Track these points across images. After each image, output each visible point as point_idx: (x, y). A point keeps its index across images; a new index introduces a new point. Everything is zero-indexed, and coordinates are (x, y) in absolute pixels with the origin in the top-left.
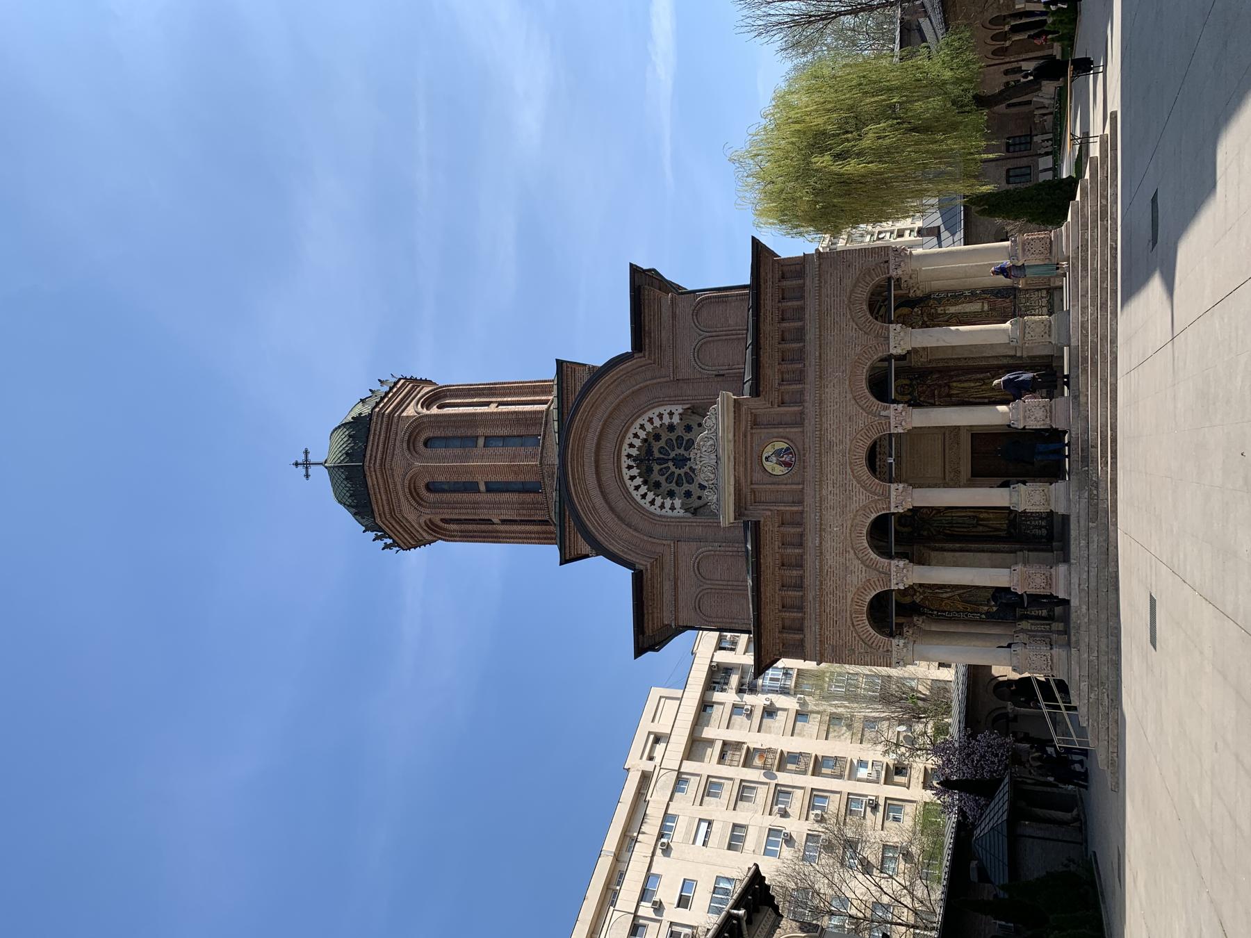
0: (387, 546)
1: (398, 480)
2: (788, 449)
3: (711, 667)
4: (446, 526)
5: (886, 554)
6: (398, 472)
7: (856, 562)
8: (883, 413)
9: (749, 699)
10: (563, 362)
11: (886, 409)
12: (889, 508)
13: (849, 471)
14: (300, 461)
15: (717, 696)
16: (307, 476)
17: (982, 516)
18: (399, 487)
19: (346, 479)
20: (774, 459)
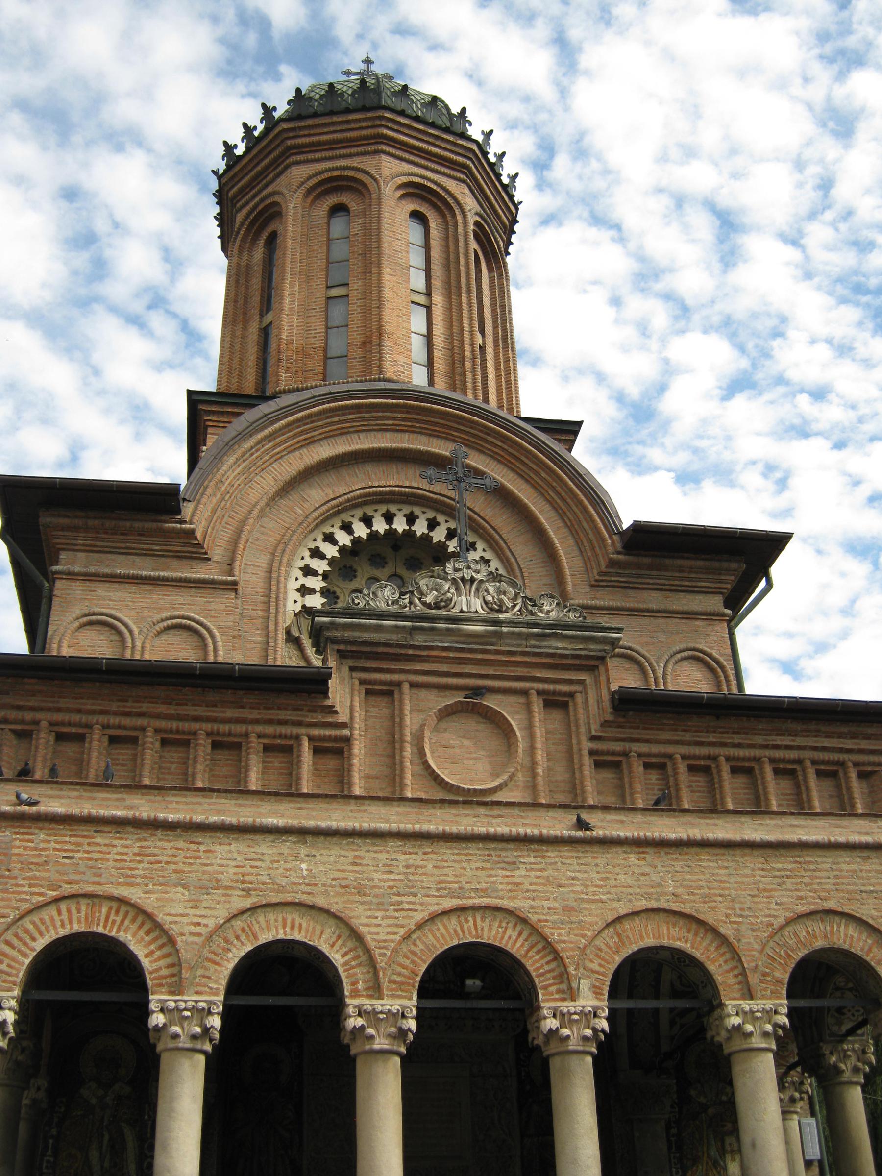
0: (229, 148)
1: (355, 162)
4: (261, 242)
6: (367, 163)
7: (222, 914)
8: (585, 986)
11: (596, 991)
12: (352, 997)
13: (448, 903)
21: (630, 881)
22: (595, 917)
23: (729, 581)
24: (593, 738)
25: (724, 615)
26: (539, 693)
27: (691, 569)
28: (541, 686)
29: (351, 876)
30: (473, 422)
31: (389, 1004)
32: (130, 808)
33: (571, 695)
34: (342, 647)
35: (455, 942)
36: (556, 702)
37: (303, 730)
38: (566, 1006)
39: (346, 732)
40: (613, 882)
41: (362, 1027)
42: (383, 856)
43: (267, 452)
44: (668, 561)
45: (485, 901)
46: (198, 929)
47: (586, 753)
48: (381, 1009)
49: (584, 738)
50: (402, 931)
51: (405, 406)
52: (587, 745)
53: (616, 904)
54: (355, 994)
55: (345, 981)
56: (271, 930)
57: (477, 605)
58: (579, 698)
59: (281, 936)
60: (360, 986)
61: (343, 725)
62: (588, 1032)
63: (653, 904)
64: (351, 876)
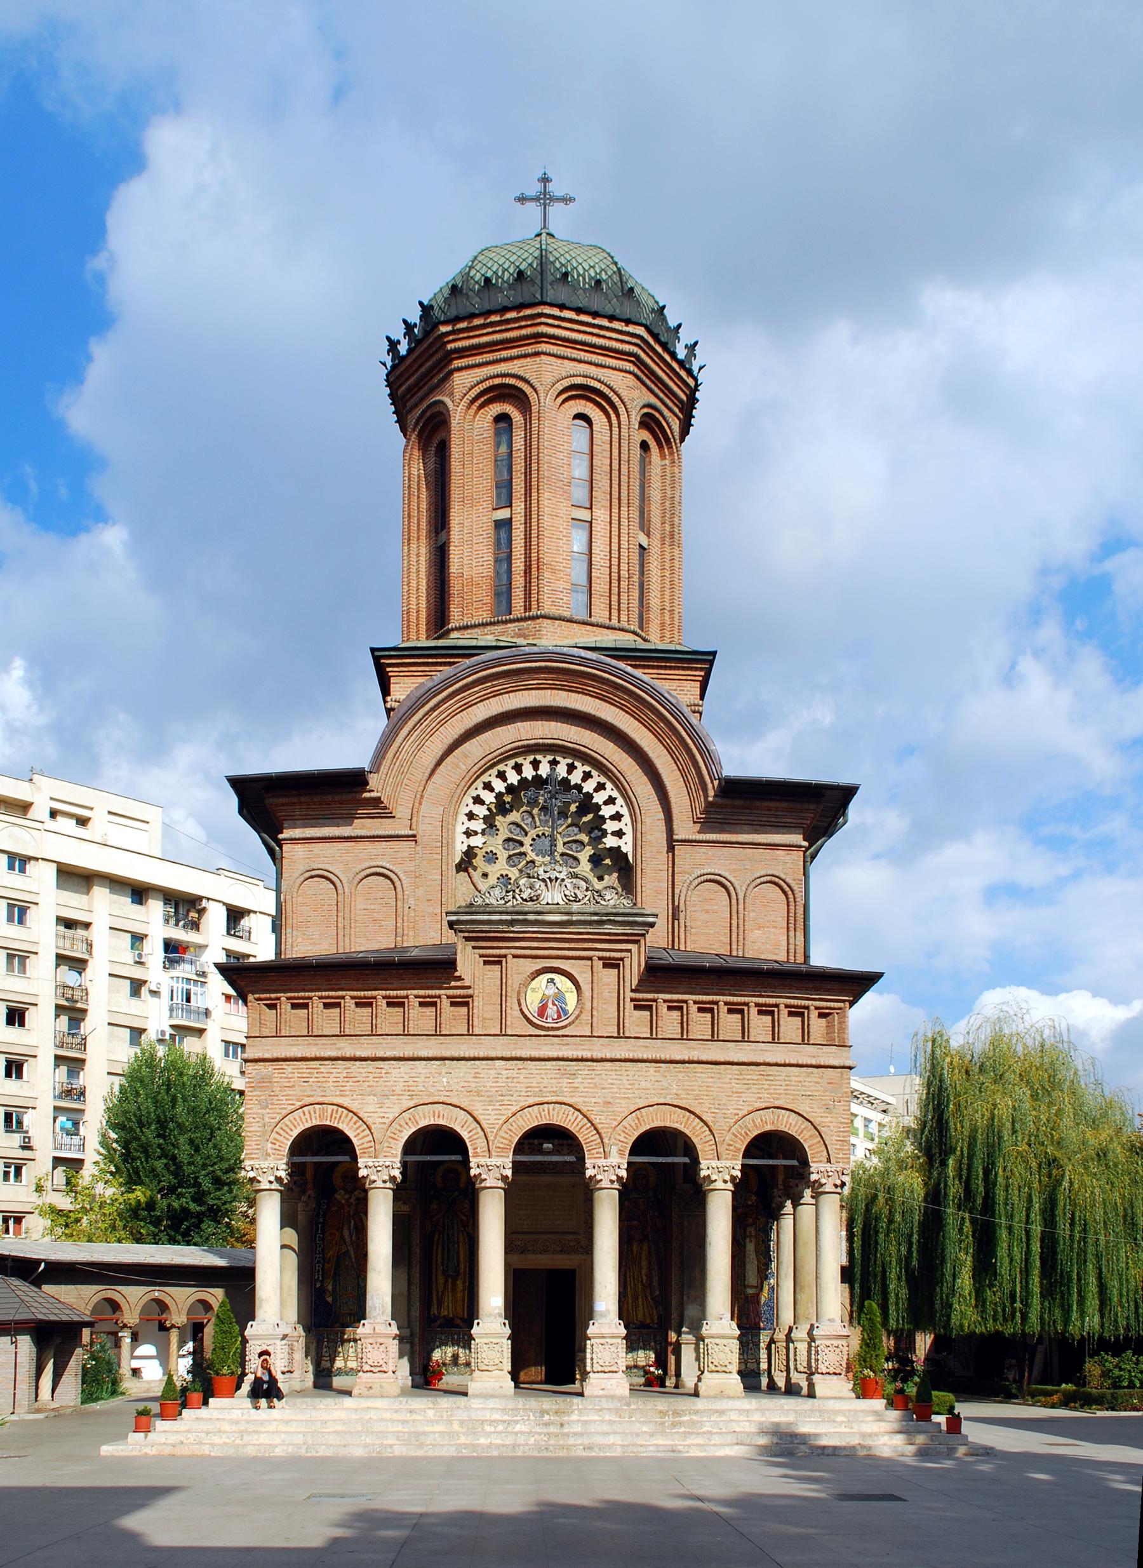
2: (565, 1012)
3: (200, 898)
5: (410, 1147)
7: (397, 1111)
8: (614, 1150)
9: (154, 951)
10: (711, 663)
13: (532, 1101)
14: (551, 187)
15: (156, 908)
16: (522, 199)
17: (459, 1283)
18: (502, 368)
19: (521, 273)
20: (551, 991)
21: (649, 1085)
22: (623, 1107)
23: (808, 819)
24: (632, 991)
25: (801, 847)
26: (600, 958)
27: (777, 809)
28: (601, 954)
29: (474, 1085)
30: (604, 679)
31: (495, 1161)
32: (339, 1049)
33: (622, 959)
34: (466, 934)
35: (536, 1124)
36: (610, 964)
37: (442, 992)
38: (601, 1162)
39: (470, 992)
40: (637, 1086)
41: (480, 1174)
42: (493, 1072)
43: (433, 721)
44: (758, 803)
45: (554, 1099)
46: (383, 1120)
47: (628, 1000)
48: (491, 1165)
49: (628, 990)
50: (504, 1118)
51: (546, 667)
52: (629, 995)
53: (638, 1100)
54: (476, 1155)
55: (470, 1148)
56: (426, 1118)
57: (559, 898)
58: (627, 962)
59: (432, 1122)
60: (478, 1150)
61: (469, 987)
62: (614, 1178)
63: (662, 1101)
64: (474, 1085)
